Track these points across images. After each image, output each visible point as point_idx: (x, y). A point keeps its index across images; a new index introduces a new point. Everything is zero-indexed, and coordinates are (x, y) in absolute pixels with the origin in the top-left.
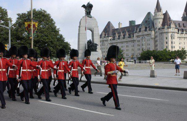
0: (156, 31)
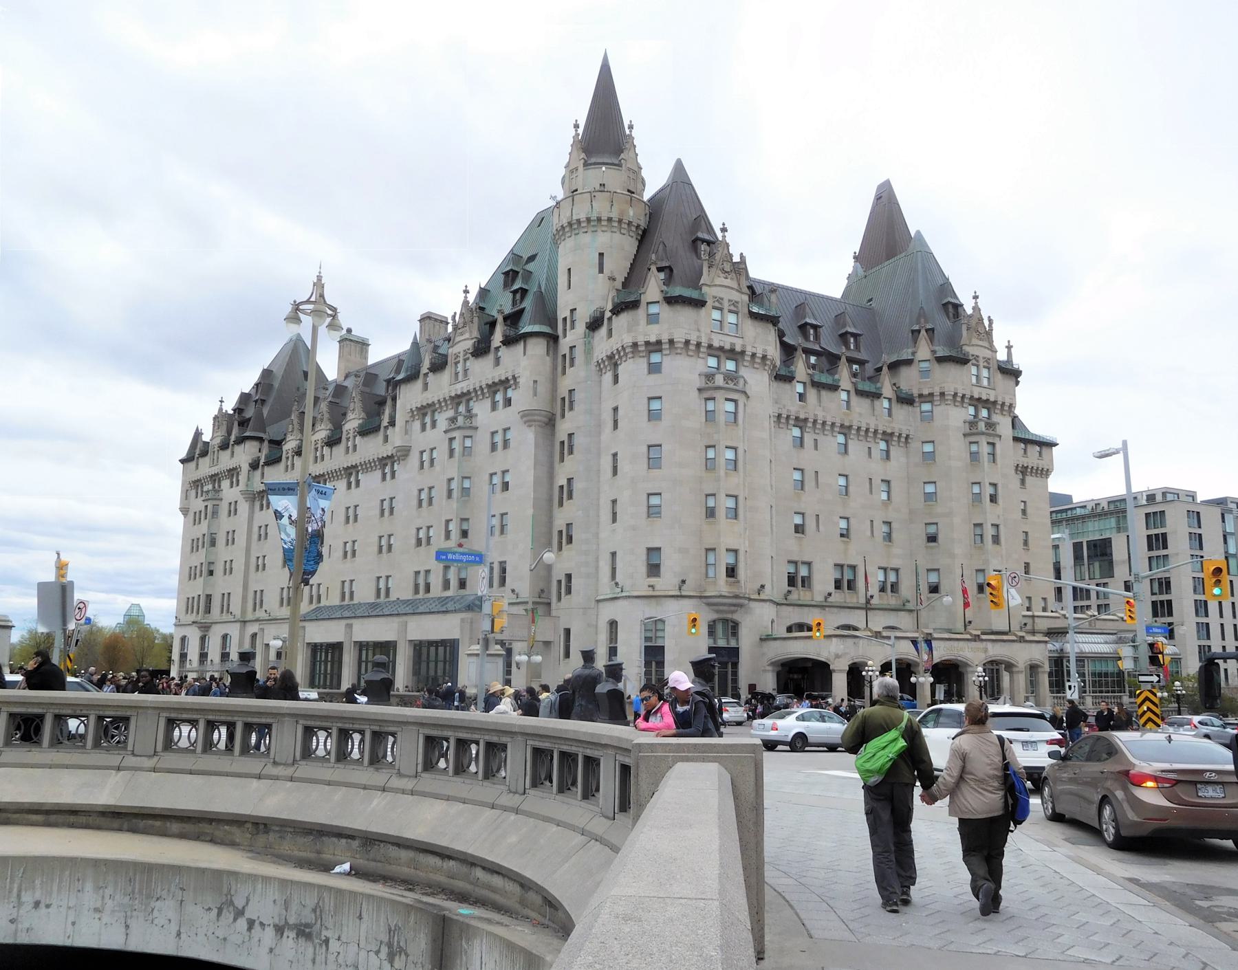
0: (564, 344)
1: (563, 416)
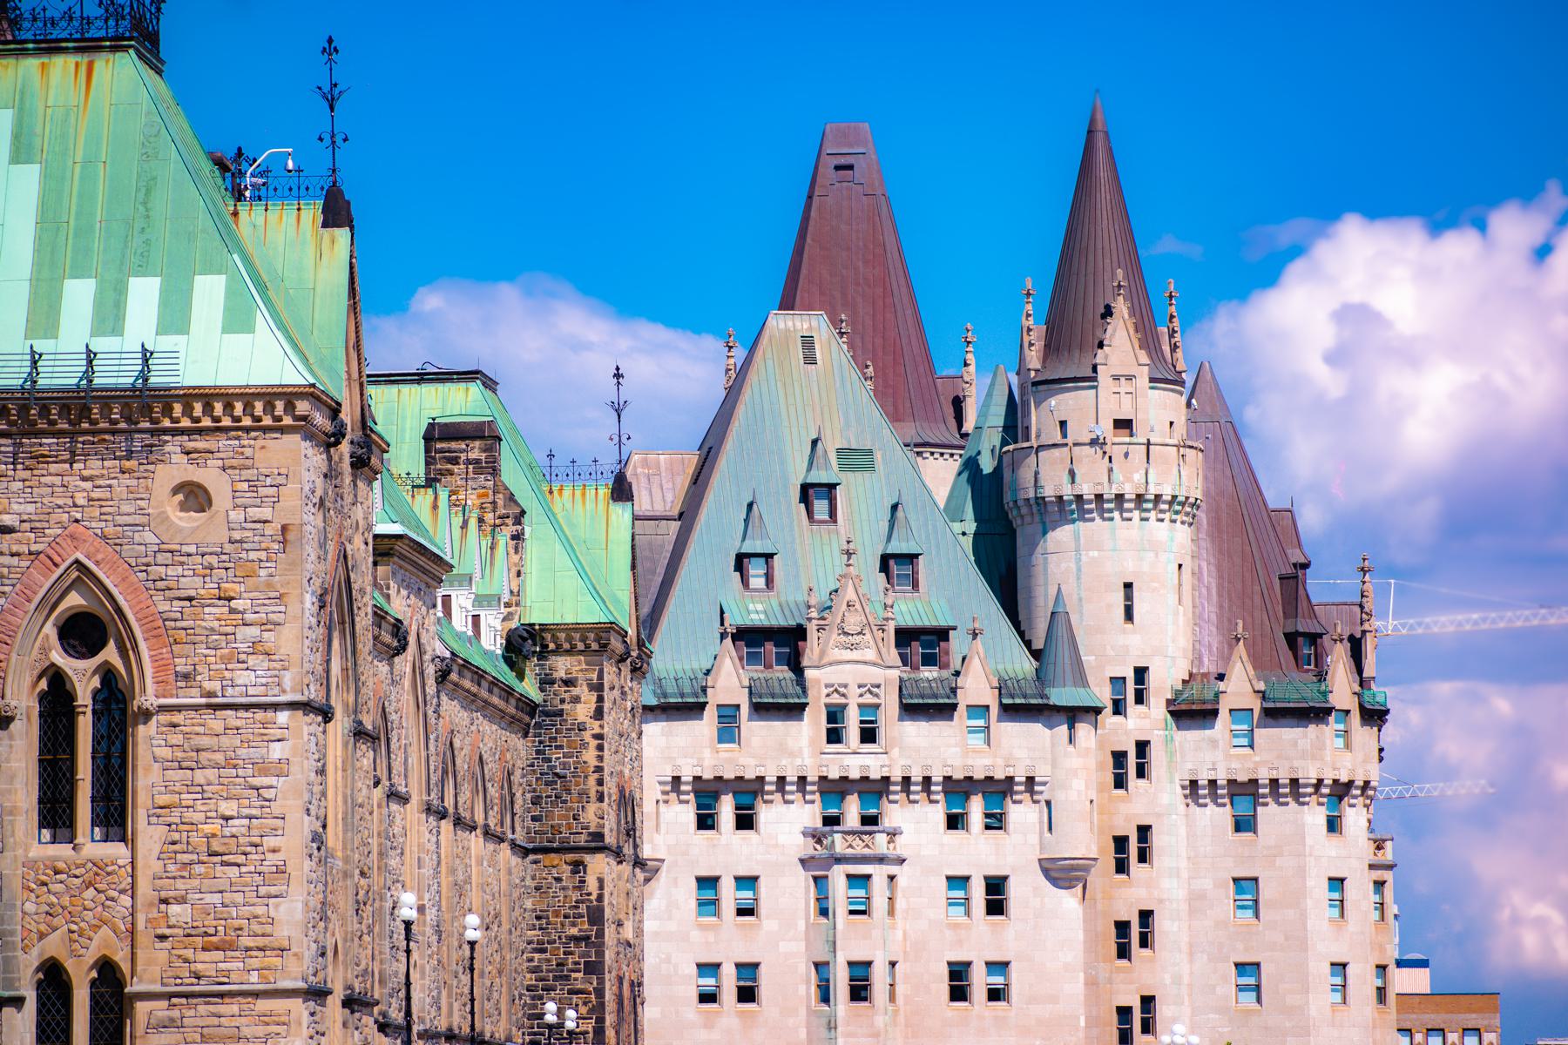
1: (1122, 867)
